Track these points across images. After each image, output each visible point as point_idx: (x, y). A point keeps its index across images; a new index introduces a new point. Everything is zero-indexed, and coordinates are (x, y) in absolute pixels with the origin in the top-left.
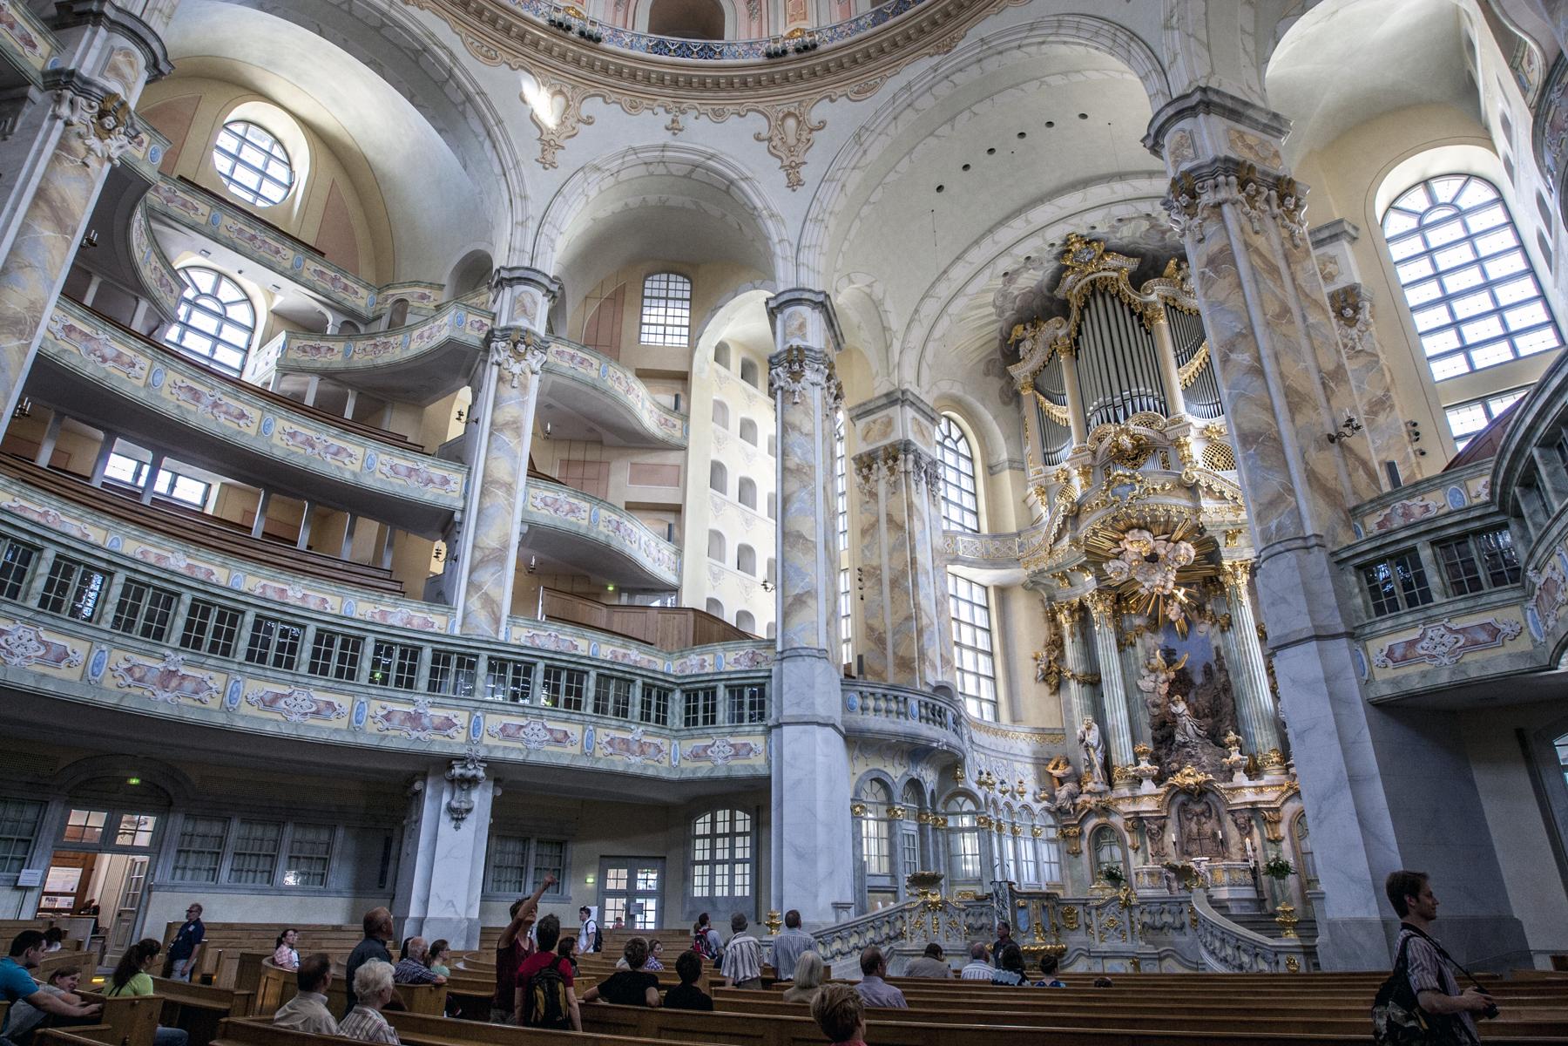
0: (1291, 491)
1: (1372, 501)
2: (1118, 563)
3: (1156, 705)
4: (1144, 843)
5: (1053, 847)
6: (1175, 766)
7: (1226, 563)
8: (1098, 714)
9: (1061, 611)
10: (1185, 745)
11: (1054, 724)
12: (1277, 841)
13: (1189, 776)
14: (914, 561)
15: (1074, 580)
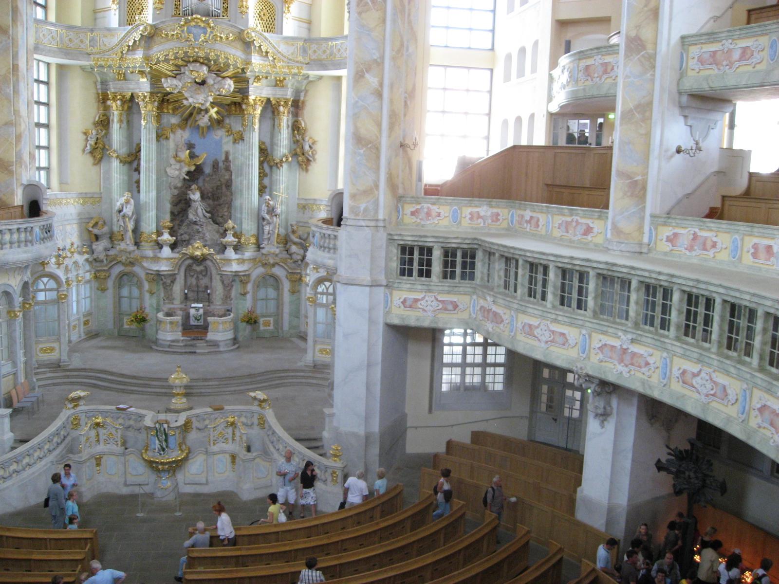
0: (377, 186)
1: (413, 197)
2: (175, 82)
3: (176, 188)
4: (158, 290)
5: (88, 286)
6: (186, 237)
7: (252, 98)
8: (134, 186)
9: (114, 99)
10: (195, 223)
11: (95, 189)
12: (244, 294)
13: (198, 249)
14: (15, 68)
15: (130, 76)
